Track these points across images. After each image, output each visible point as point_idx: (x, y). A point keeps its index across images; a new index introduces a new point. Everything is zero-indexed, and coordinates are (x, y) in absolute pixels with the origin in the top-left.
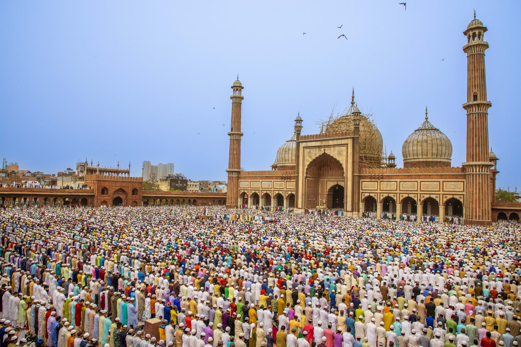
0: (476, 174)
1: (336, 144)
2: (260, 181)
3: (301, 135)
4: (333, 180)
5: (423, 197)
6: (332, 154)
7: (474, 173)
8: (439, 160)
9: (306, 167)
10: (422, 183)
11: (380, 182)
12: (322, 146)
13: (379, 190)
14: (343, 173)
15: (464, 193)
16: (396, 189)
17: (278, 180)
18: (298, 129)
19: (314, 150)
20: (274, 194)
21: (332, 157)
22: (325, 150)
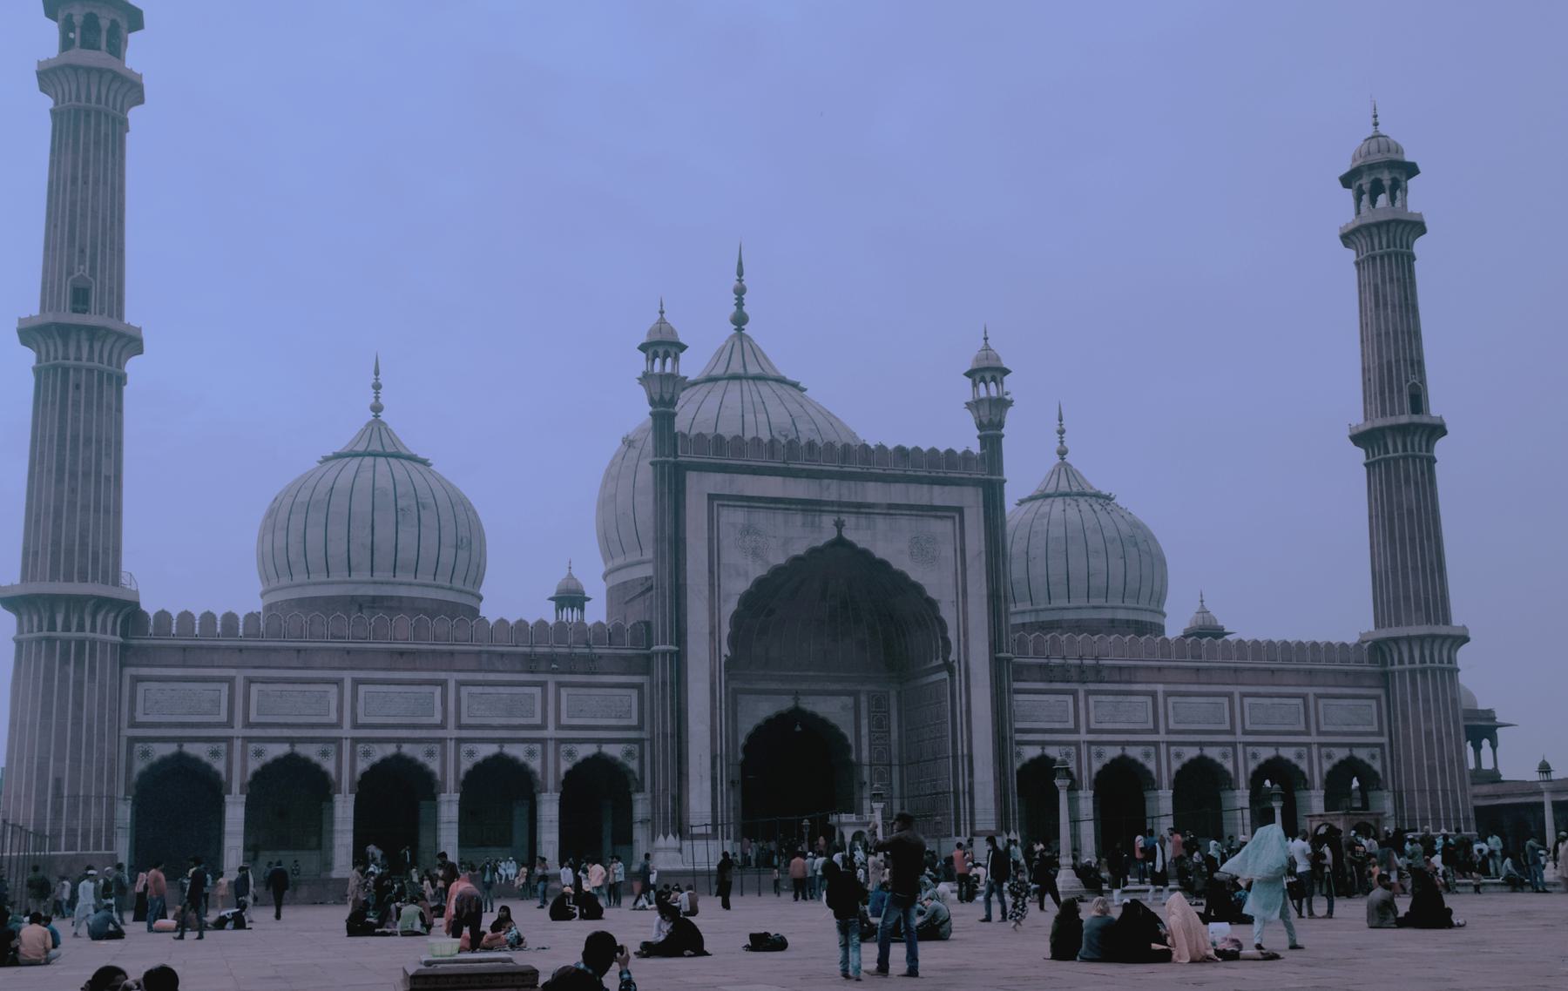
0: (1443, 670)
1: (904, 501)
2: (338, 682)
4: (773, 686)
5: (1254, 756)
6: (881, 551)
7: (1437, 664)
9: (730, 607)
11: (1088, 693)
12: (826, 503)
13: (1083, 729)
15: (1385, 740)
16: (1151, 725)
17: (492, 677)
19: (780, 517)
20: (466, 765)
21: (884, 565)
22: (839, 525)
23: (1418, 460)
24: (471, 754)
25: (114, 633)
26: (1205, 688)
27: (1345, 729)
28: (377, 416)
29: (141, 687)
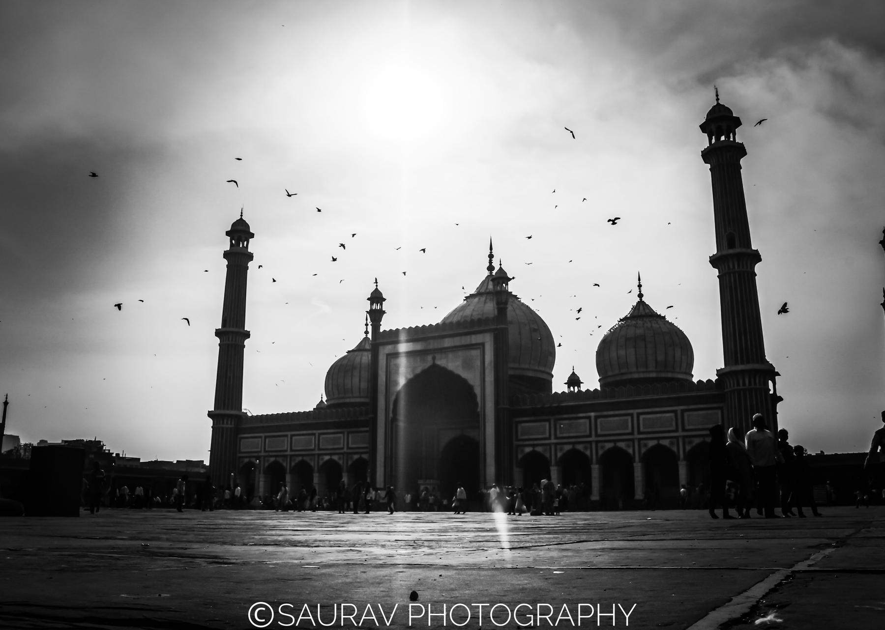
2: (286, 436)
3: (381, 330)
5: (645, 445)
7: (741, 387)
8: (670, 375)
10: (642, 417)
11: (556, 420)
12: (430, 350)
13: (553, 437)
14: (477, 404)
16: (588, 432)
18: (376, 316)
21: (451, 373)
22: (434, 359)
23: (732, 275)
24: (322, 459)
25: (231, 424)
26: (617, 412)
27: (700, 427)
28: (367, 336)
29: (243, 441)
